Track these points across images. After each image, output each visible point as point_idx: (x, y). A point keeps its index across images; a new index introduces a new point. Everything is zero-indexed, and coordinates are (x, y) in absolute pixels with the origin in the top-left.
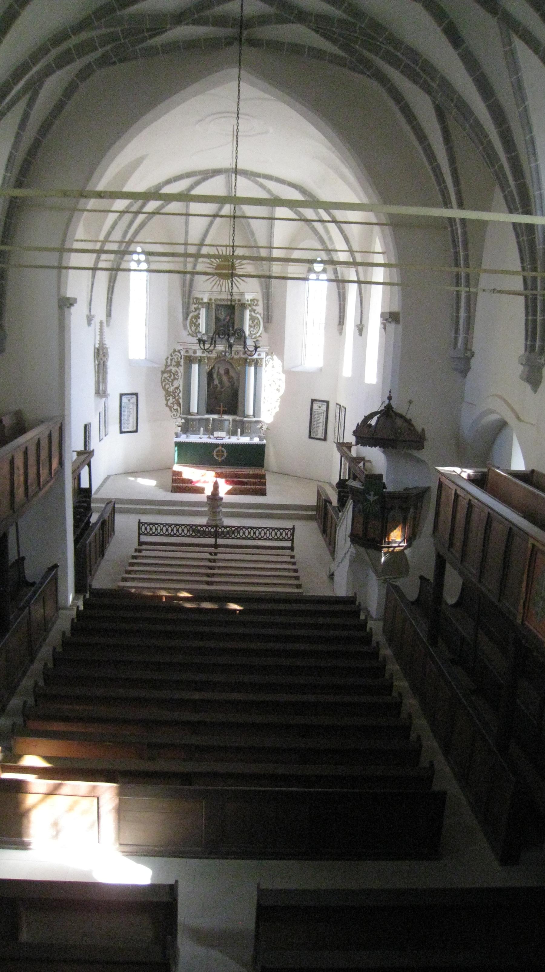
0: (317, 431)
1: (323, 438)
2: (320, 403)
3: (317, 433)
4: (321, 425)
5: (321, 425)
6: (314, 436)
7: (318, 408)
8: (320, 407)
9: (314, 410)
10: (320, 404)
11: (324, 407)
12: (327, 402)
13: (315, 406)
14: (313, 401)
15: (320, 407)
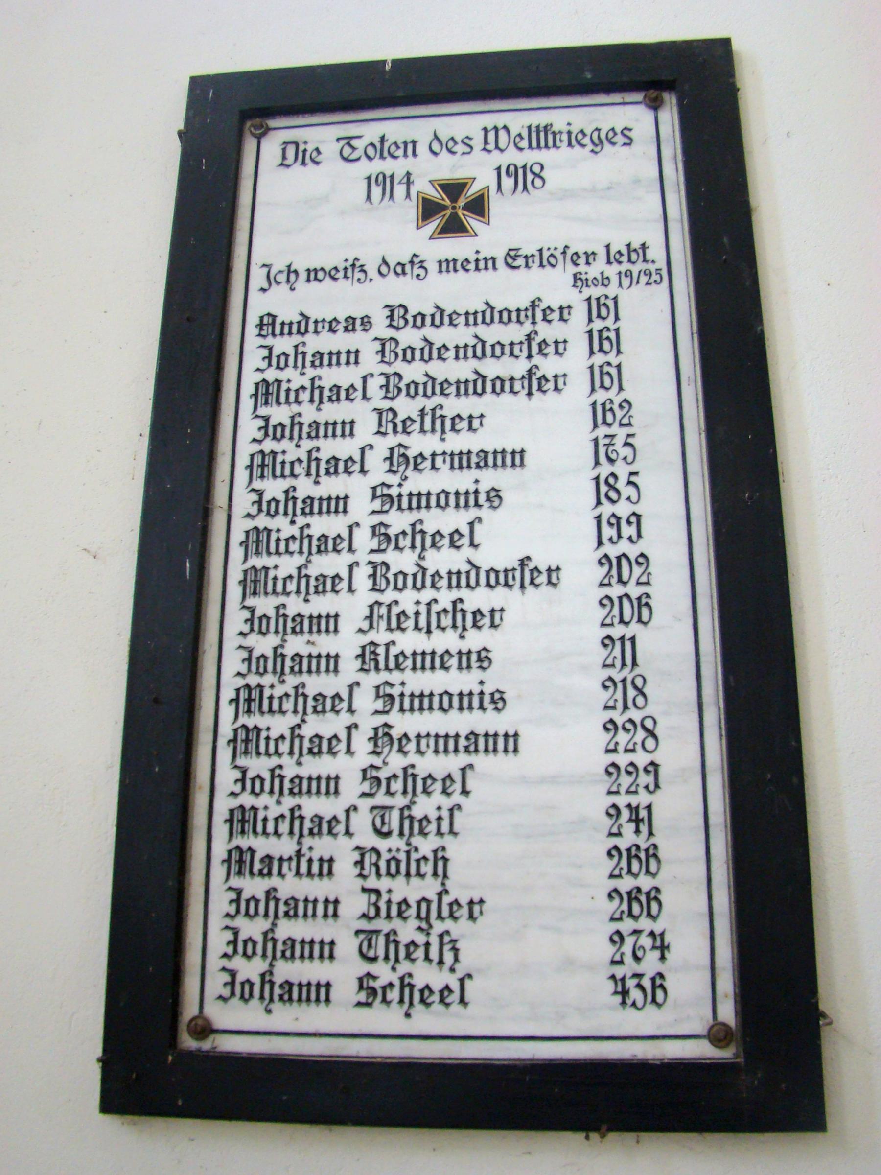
0: (412, 833)
1: (687, 1013)
2: (464, 122)
3: (415, 927)
4: (545, 648)
5: (545, 648)
6: (341, 1025)
7: (399, 232)
8: (452, 209)
9: (255, 301)
10: (450, 142)
11: (615, 180)
12: (694, 84)
13: (306, 204)
14: (230, 117)
15: (452, 209)
